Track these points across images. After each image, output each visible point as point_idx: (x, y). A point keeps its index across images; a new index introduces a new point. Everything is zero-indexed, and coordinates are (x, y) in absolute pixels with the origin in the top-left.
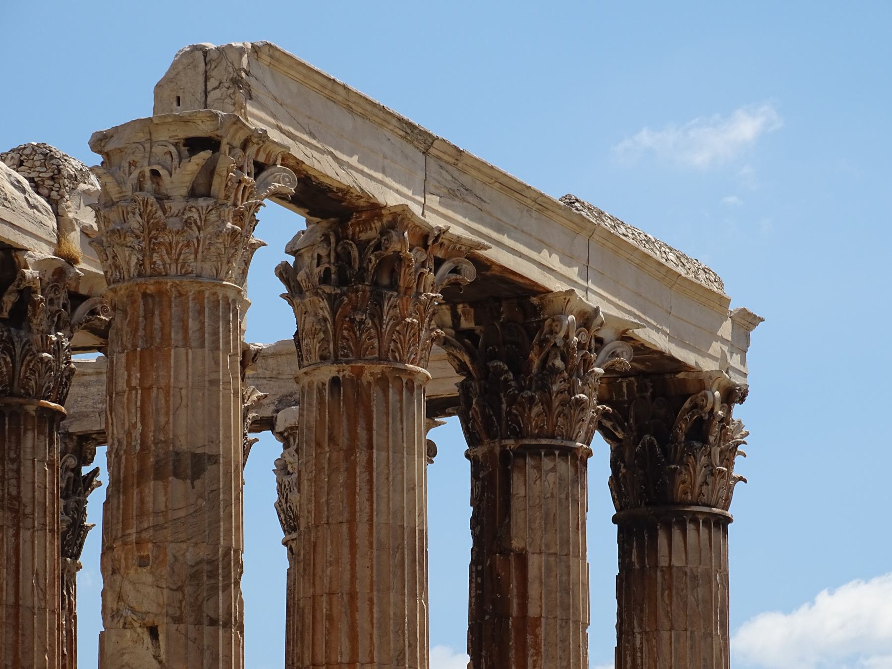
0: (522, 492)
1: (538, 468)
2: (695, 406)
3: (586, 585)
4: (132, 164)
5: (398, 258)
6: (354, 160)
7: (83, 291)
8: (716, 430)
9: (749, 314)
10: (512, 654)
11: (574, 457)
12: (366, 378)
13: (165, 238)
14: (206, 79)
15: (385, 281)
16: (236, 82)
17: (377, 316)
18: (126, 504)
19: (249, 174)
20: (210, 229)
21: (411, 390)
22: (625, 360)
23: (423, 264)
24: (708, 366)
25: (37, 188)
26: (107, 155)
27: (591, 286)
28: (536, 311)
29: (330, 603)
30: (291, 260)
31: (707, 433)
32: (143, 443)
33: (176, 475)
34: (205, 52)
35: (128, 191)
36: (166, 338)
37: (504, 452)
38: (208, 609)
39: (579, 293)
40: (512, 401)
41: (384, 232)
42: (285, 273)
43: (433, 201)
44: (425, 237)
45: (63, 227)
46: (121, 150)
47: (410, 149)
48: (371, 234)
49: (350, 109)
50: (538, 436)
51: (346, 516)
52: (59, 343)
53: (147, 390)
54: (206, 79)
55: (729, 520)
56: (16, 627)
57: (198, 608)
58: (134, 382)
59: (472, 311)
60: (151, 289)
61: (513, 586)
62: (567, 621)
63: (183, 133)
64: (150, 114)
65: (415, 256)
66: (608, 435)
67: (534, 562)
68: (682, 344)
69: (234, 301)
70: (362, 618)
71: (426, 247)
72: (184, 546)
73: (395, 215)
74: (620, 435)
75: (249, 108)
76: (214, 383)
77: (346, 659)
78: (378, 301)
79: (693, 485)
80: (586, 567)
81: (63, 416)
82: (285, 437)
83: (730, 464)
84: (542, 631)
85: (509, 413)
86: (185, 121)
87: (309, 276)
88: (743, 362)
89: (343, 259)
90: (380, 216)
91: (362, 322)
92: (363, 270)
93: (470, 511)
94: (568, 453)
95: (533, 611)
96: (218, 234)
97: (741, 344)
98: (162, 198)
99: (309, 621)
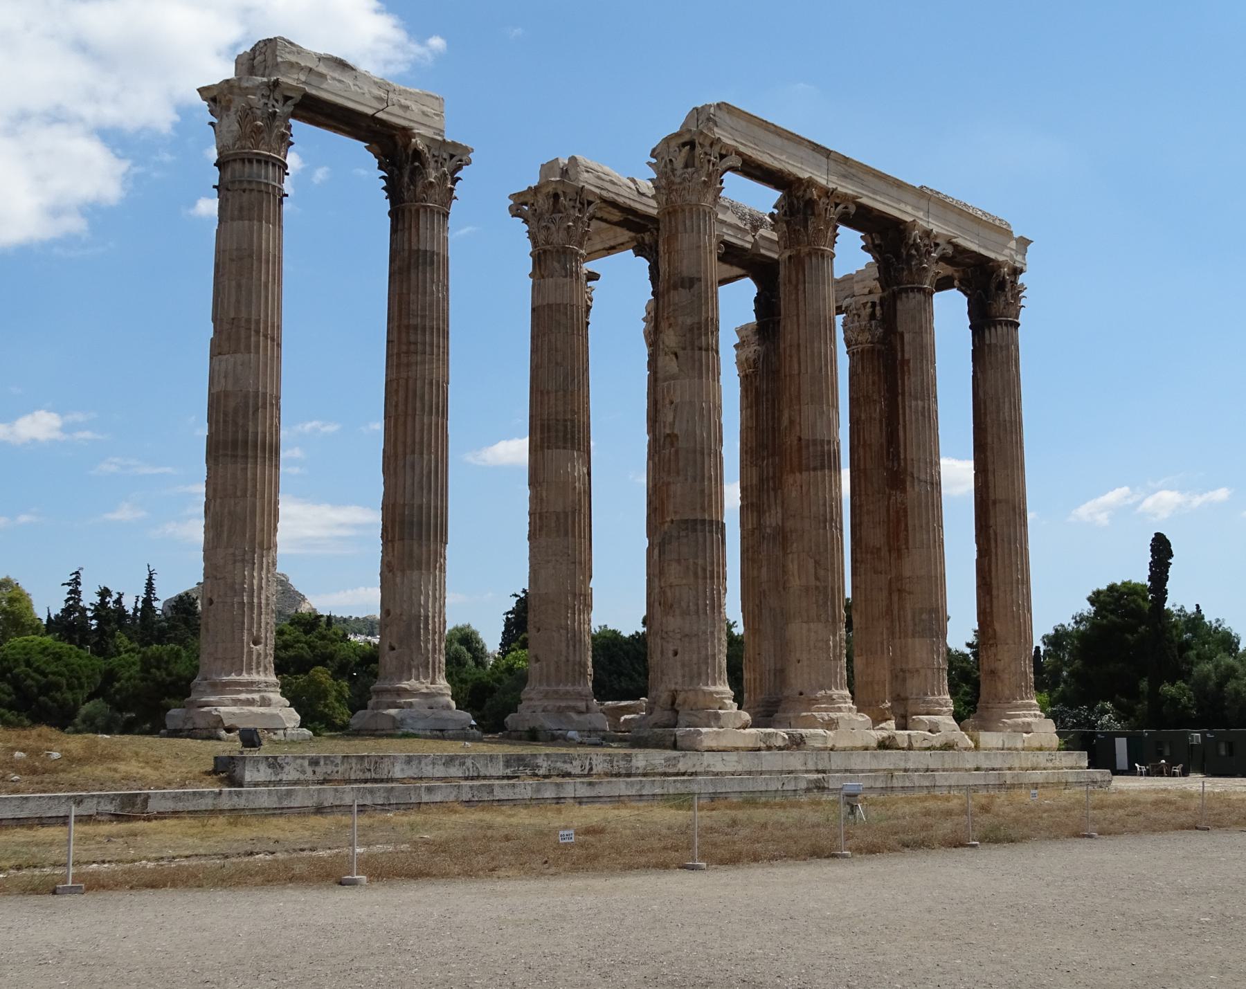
6: (783, 158)
8: (1009, 286)
9: (1024, 238)
10: (899, 375)
13: (674, 187)
14: (698, 121)
15: (809, 212)
16: (709, 119)
17: (806, 227)
19: (716, 158)
22: (950, 251)
24: (1001, 258)
27: (930, 220)
30: (776, 211)
32: (669, 276)
33: (683, 287)
36: (677, 229)
43: (834, 178)
49: (779, 135)
51: (795, 313)
53: (670, 253)
54: (698, 121)
57: (692, 343)
59: (878, 236)
62: (922, 360)
67: (907, 337)
68: (987, 249)
69: (709, 213)
74: (969, 292)
78: (806, 220)
88: (1024, 259)
89: (791, 205)
90: (803, 184)
91: (799, 230)
92: (798, 207)
95: (907, 356)
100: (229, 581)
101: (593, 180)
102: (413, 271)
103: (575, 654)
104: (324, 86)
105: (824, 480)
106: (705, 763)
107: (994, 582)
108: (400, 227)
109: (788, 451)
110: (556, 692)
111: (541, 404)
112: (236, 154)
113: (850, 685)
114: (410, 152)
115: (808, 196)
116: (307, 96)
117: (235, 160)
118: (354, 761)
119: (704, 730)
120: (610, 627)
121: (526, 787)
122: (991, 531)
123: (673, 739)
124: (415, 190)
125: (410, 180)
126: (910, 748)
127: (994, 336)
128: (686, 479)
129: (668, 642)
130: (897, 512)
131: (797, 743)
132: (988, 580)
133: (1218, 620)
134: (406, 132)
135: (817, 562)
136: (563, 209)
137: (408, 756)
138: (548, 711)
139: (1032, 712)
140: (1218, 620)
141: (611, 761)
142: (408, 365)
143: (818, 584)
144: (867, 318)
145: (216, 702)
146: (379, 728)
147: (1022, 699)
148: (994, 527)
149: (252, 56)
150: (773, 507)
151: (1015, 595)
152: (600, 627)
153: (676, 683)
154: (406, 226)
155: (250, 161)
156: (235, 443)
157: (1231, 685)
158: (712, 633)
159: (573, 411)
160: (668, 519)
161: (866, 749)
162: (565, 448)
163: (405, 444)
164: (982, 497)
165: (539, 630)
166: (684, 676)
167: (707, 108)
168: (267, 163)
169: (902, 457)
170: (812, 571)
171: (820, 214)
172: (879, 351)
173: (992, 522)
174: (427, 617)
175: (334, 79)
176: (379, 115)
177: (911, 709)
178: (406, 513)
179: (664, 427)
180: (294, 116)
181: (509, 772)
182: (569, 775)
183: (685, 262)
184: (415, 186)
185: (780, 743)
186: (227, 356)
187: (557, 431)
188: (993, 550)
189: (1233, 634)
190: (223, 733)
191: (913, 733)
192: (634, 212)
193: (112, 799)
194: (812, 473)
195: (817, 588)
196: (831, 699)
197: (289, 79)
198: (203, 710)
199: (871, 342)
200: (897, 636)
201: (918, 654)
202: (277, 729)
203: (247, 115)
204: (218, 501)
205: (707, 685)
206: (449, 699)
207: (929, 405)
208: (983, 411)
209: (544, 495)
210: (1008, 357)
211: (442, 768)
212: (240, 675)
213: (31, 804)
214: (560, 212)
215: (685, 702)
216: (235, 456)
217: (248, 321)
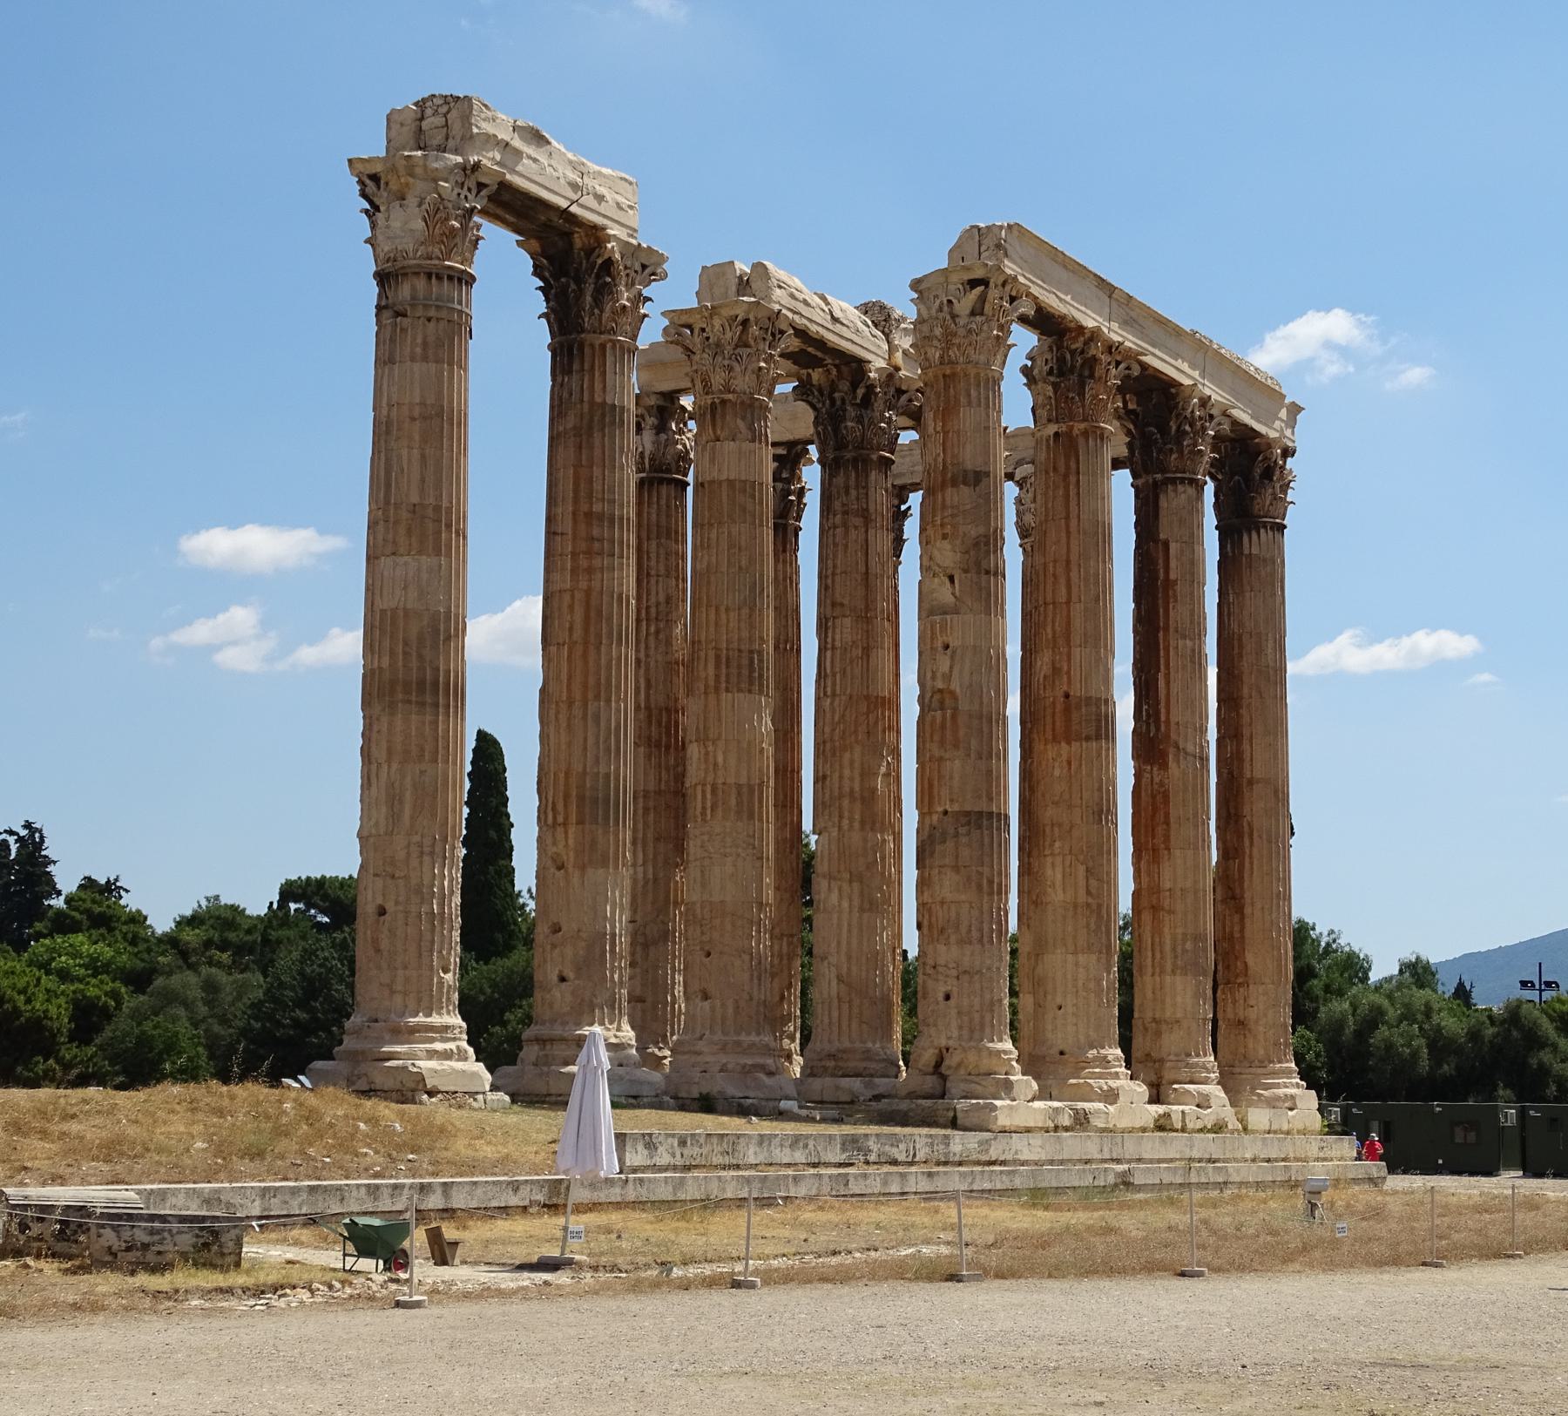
0: (1166, 505)
1: (1175, 491)
2: (1266, 458)
3: (1204, 561)
4: (936, 297)
5: (1094, 359)
6: (1068, 298)
7: (904, 388)
8: (1278, 473)
10: (1160, 602)
11: (1197, 484)
12: (1076, 432)
15: (1086, 373)
16: (998, 246)
17: (1082, 394)
18: (935, 502)
20: (983, 335)
21: (1102, 439)
22: (1226, 427)
23: (1109, 364)
24: (1273, 434)
25: (876, 325)
26: (920, 292)
28: (1174, 396)
29: (1054, 567)
30: (1029, 363)
31: (1273, 475)
33: (965, 483)
35: (933, 312)
36: (957, 401)
37: (1155, 483)
38: (984, 565)
39: (1200, 387)
40: (1160, 451)
41: (1086, 343)
42: (1025, 371)
43: (1115, 326)
44: (1111, 347)
45: (892, 349)
47: (1101, 293)
48: (1078, 345)
49: (1065, 267)
50: (1175, 472)
51: (1064, 515)
52: (890, 418)
53: (946, 433)
55: (1285, 527)
56: (867, 586)
57: (978, 564)
58: (939, 429)
60: (948, 372)
61: (1161, 561)
64: (945, 265)
65: (1104, 358)
66: (1213, 478)
67: (1173, 547)
70: (1074, 575)
71: (1111, 353)
73: (1093, 333)
74: (1220, 477)
75: (1006, 262)
76: (987, 428)
77: (1064, 600)
78: (1082, 385)
80: (1204, 550)
81: (893, 462)
82: (1020, 484)
83: (1286, 494)
84: (1178, 588)
85: (1158, 459)
86: (967, 269)
87: (1040, 372)
88: (1293, 433)
89: (1061, 360)
90: (1083, 334)
92: (1073, 367)
93: (1134, 518)
94: (1193, 482)
95: (1172, 576)
96: (988, 338)
97: (1292, 422)
98: (954, 317)
99: (1042, 578)
100: (414, 881)
101: (787, 301)
103: (760, 989)
104: (519, 168)
105: (1099, 755)
106: (1013, 1151)
107: (1247, 895)
108: (576, 367)
109: (1049, 711)
110: (738, 1043)
111: (716, 624)
113: (1126, 1044)
114: (599, 261)
115: (1092, 352)
116: (504, 186)
117: (417, 274)
118: (715, 1140)
119: (998, 1103)
120: (224, 900)
121: (873, 1179)
122: (1245, 824)
123: (951, 1114)
124: (600, 316)
126: (1183, 1130)
127: (1254, 544)
128: (969, 755)
129: (937, 980)
130: (1153, 797)
131: (1081, 1121)
132: (1238, 891)
133: (1332, 932)
134: (596, 234)
135: (1087, 870)
136: (752, 343)
137: (761, 1136)
139: (1294, 1081)
140: (1332, 932)
141: (932, 1144)
142: (590, 571)
143: (1090, 900)
145: (405, 1054)
146: (553, 1091)
147: (1280, 1062)
148: (1249, 818)
149: (419, 116)
151: (1274, 915)
152: (208, 899)
153: (949, 1038)
154: (586, 366)
155: (439, 278)
156: (421, 684)
157: (1383, 1032)
158: (998, 969)
159: (761, 638)
160: (940, 809)
161: (1144, 1130)
162: (750, 691)
163: (585, 686)
164: (1231, 773)
165: (708, 954)
166: (960, 1028)
167: (996, 231)
168: (460, 280)
169: (1163, 718)
170: (1082, 882)
171: (1100, 378)
173: (1246, 810)
174: (613, 935)
175: (529, 157)
176: (574, 209)
177: (1168, 1075)
178: (588, 785)
179: (933, 678)
180: (484, 212)
181: (842, 1158)
182: (895, 1162)
183: (969, 448)
185: (1066, 1121)
186: (406, 558)
187: (739, 667)
188: (1247, 851)
189: (1362, 956)
190: (425, 1097)
191: (1186, 1108)
192: (821, 344)
193: (541, 1184)
194: (1084, 744)
195: (1088, 905)
196: (1104, 1062)
197: (489, 159)
198: (387, 1064)
200: (1150, 970)
201: (1179, 999)
202: (477, 1093)
203: (435, 214)
204: (395, 766)
205: (993, 1041)
206: (634, 1051)
207: (1200, 646)
208: (1236, 651)
209: (720, 759)
210: (1273, 574)
211: (787, 1151)
212: (430, 1015)
213: (479, 1191)
214: (747, 345)
215: (959, 1065)
216: (422, 704)
217: (437, 509)
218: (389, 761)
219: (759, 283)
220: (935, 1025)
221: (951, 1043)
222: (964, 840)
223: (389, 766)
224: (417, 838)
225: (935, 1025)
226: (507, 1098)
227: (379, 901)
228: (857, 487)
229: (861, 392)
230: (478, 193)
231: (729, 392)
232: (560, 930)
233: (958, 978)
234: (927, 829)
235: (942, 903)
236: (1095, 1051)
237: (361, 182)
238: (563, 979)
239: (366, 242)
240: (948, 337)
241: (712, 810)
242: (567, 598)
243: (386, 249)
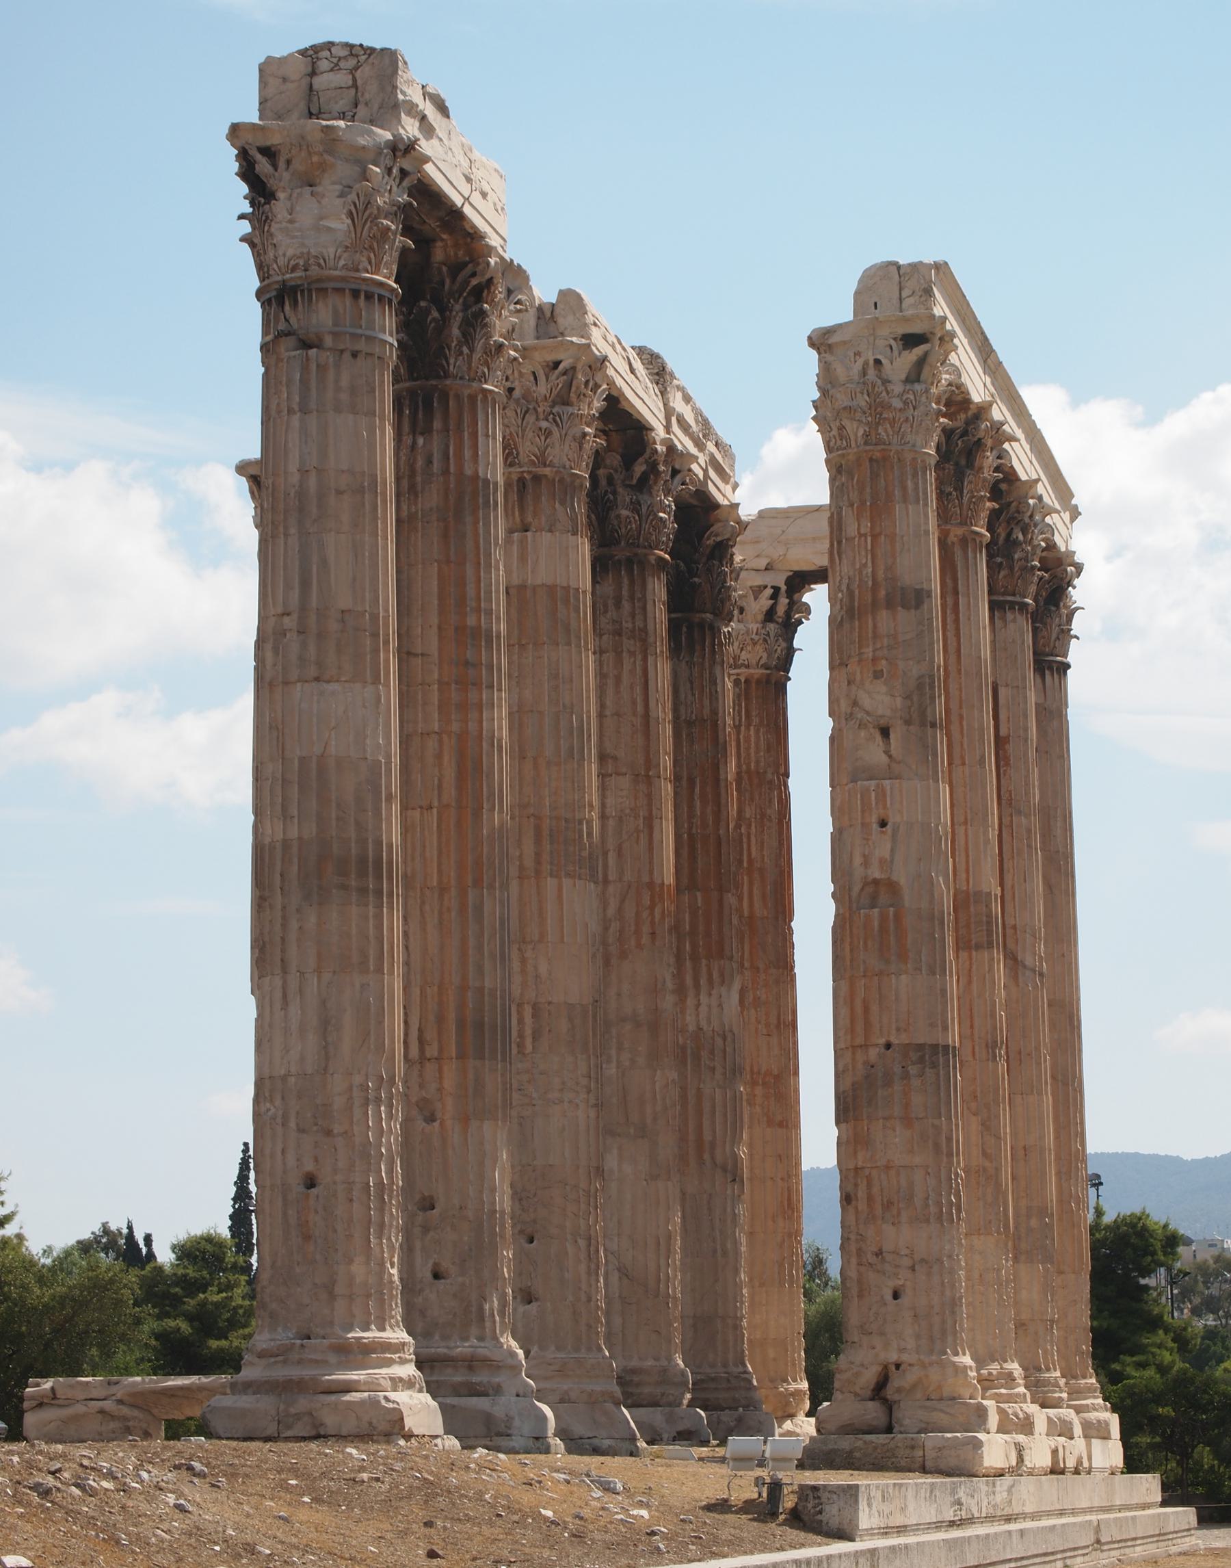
4: (857, 354)
14: (900, 290)
17: (960, 489)
20: (922, 408)
34: (899, 267)
46: (845, 343)
50: (1004, 594)
55: (1068, 666)
57: (923, 714)
60: (877, 455)
63: (903, 330)
72: (911, 663)
79: (1049, 638)
86: (907, 320)
90: (967, 409)
91: (950, 494)
98: (886, 382)
102: (469, 519)
108: (437, 424)
112: (343, 279)
124: (470, 357)
125: (464, 334)
138: (569, 1401)
144: (760, 617)
145: (366, 1383)
150: (691, 993)
153: (902, 1350)
160: (882, 1041)
172: (758, 682)
176: (467, 210)
184: (472, 350)
194: (974, 953)
198: (348, 1397)
199: (766, 666)
204: (327, 977)
215: (914, 1387)
216: (363, 891)
218: (318, 971)
219: (570, 318)
220: (882, 1334)
221: (905, 1357)
222: (916, 1082)
223: (319, 978)
224: (357, 1079)
225: (882, 1334)
226: (456, 1443)
227: (309, 1167)
228: (632, 598)
229: (639, 468)
230: (402, 180)
231: (545, 465)
232: (433, 1208)
233: (913, 1269)
234: (860, 1066)
235: (888, 1167)
236: (996, 1366)
237: (244, 156)
238: (437, 1276)
239: (242, 240)
240: (878, 409)
241: (535, 1039)
242: (432, 744)
243: (290, 252)
